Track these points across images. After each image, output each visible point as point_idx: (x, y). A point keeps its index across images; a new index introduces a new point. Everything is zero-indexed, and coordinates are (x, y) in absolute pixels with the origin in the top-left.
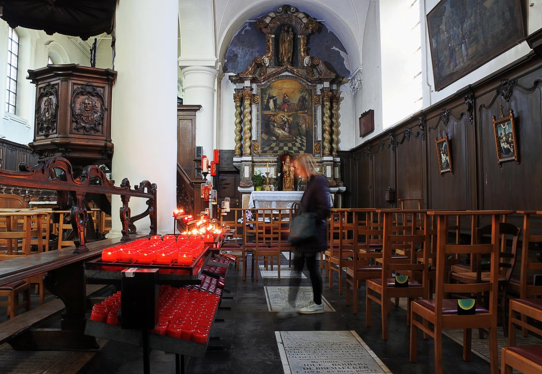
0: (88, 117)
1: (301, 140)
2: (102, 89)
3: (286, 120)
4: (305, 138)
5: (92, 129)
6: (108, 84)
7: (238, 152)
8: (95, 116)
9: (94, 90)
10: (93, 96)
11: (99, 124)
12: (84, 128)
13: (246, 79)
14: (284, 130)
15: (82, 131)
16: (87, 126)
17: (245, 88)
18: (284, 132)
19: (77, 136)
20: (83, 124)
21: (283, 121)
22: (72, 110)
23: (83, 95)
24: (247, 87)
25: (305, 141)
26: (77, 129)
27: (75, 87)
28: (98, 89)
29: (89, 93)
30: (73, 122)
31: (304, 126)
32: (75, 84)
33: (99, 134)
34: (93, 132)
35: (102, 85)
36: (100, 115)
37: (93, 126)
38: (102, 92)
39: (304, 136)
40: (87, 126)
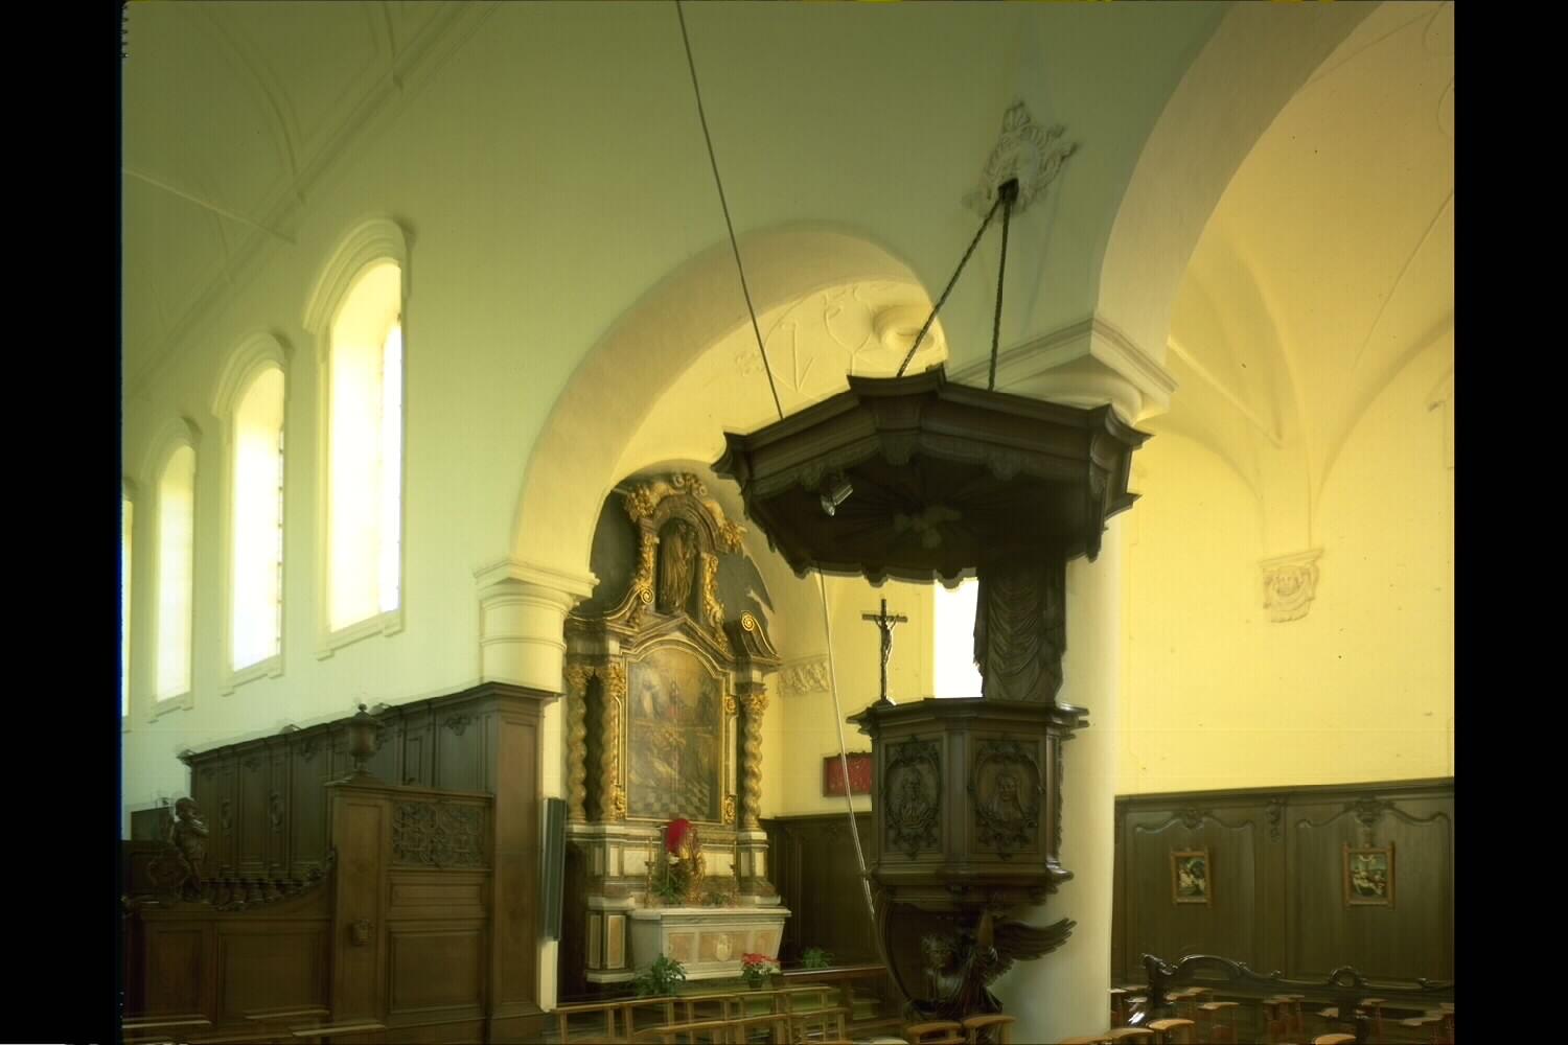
1: (701, 791)
3: (674, 743)
4: (707, 786)
14: (670, 764)
18: (669, 770)
21: (670, 744)
24: (615, 656)
25: (706, 792)
31: (705, 760)
39: (706, 783)
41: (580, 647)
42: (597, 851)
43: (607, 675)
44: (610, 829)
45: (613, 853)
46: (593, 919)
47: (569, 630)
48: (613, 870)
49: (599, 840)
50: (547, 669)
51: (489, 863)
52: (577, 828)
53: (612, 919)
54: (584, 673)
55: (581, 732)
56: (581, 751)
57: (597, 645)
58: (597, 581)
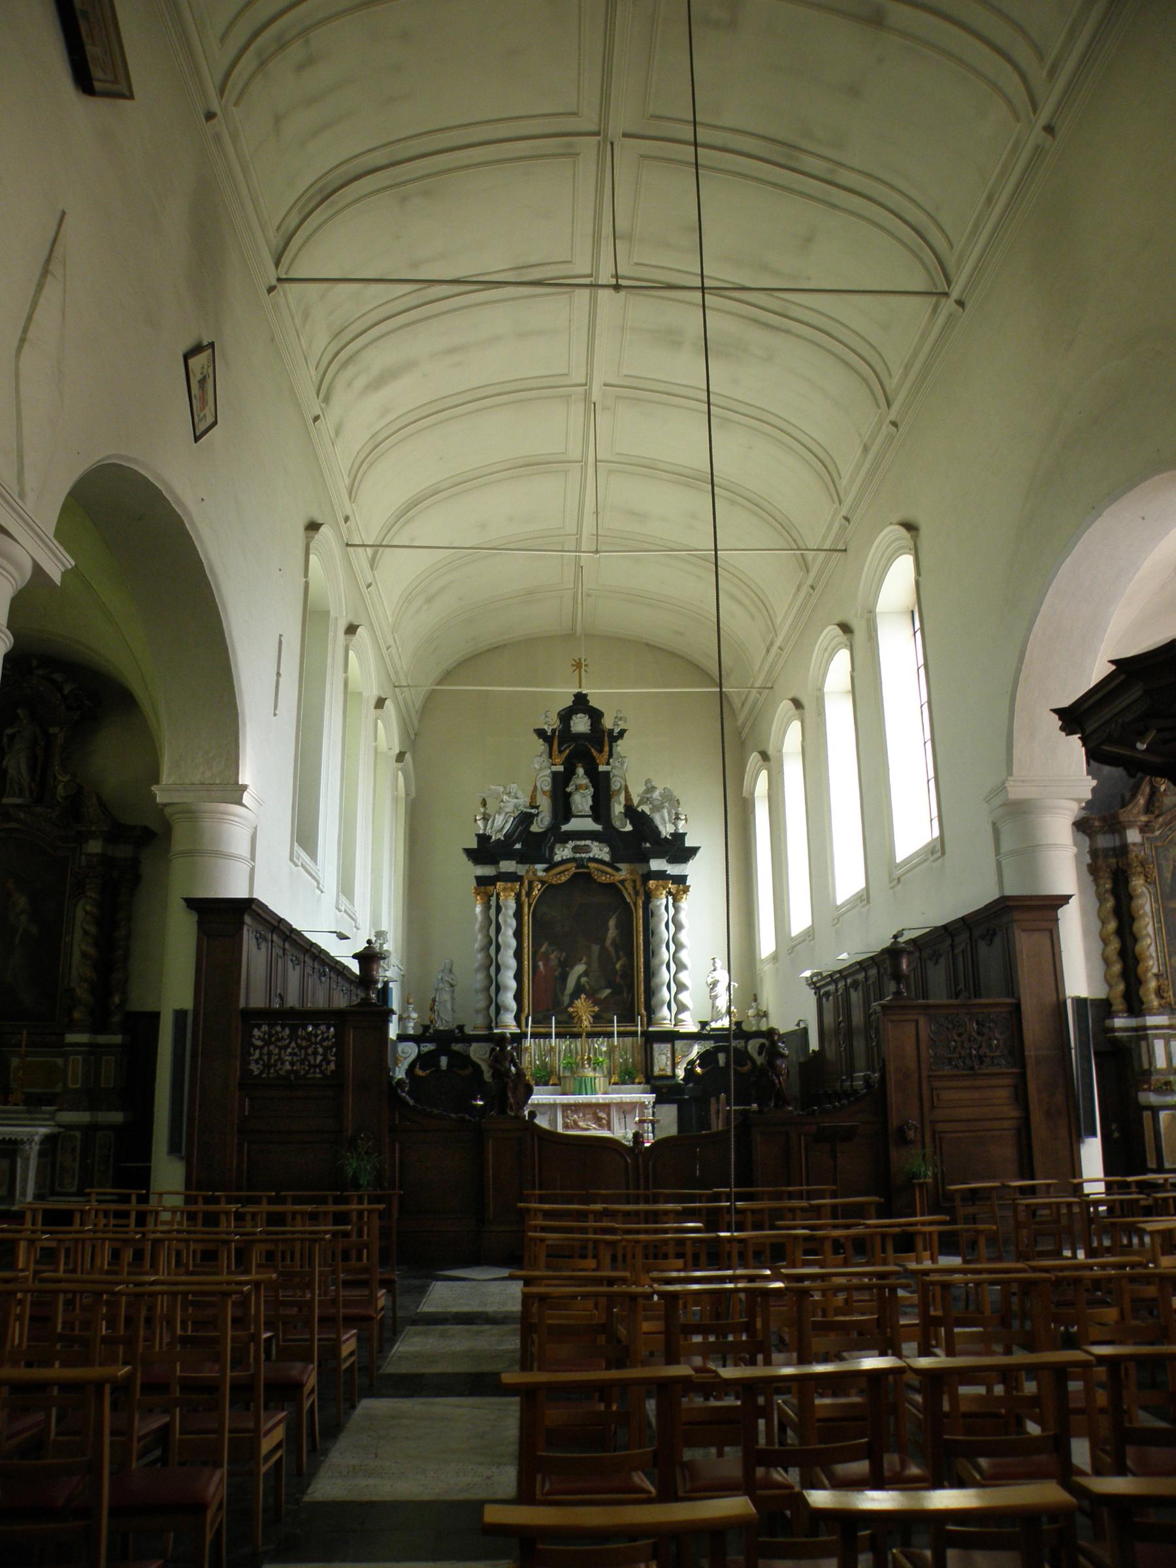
7: (1118, 1004)
13: (1131, 825)
17: (1131, 847)
24: (1134, 844)
41: (1104, 841)
42: (1143, 1044)
43: (1129, 865)
44: (1151, 1021)
45: (1159, 1046)
46: (1147, 1115)
47: (1081, 826)
48: (1161, 1063)
49: (1141, 1034)
50: (1063, 870)
51: (1021, 1062)
52: (1119, 1022)
53: (1163, 1115)
54: (1108, 866)
55: (1112, 925)
56: (1115, 945)
57: (1117, 837)
58: (1094, 783)
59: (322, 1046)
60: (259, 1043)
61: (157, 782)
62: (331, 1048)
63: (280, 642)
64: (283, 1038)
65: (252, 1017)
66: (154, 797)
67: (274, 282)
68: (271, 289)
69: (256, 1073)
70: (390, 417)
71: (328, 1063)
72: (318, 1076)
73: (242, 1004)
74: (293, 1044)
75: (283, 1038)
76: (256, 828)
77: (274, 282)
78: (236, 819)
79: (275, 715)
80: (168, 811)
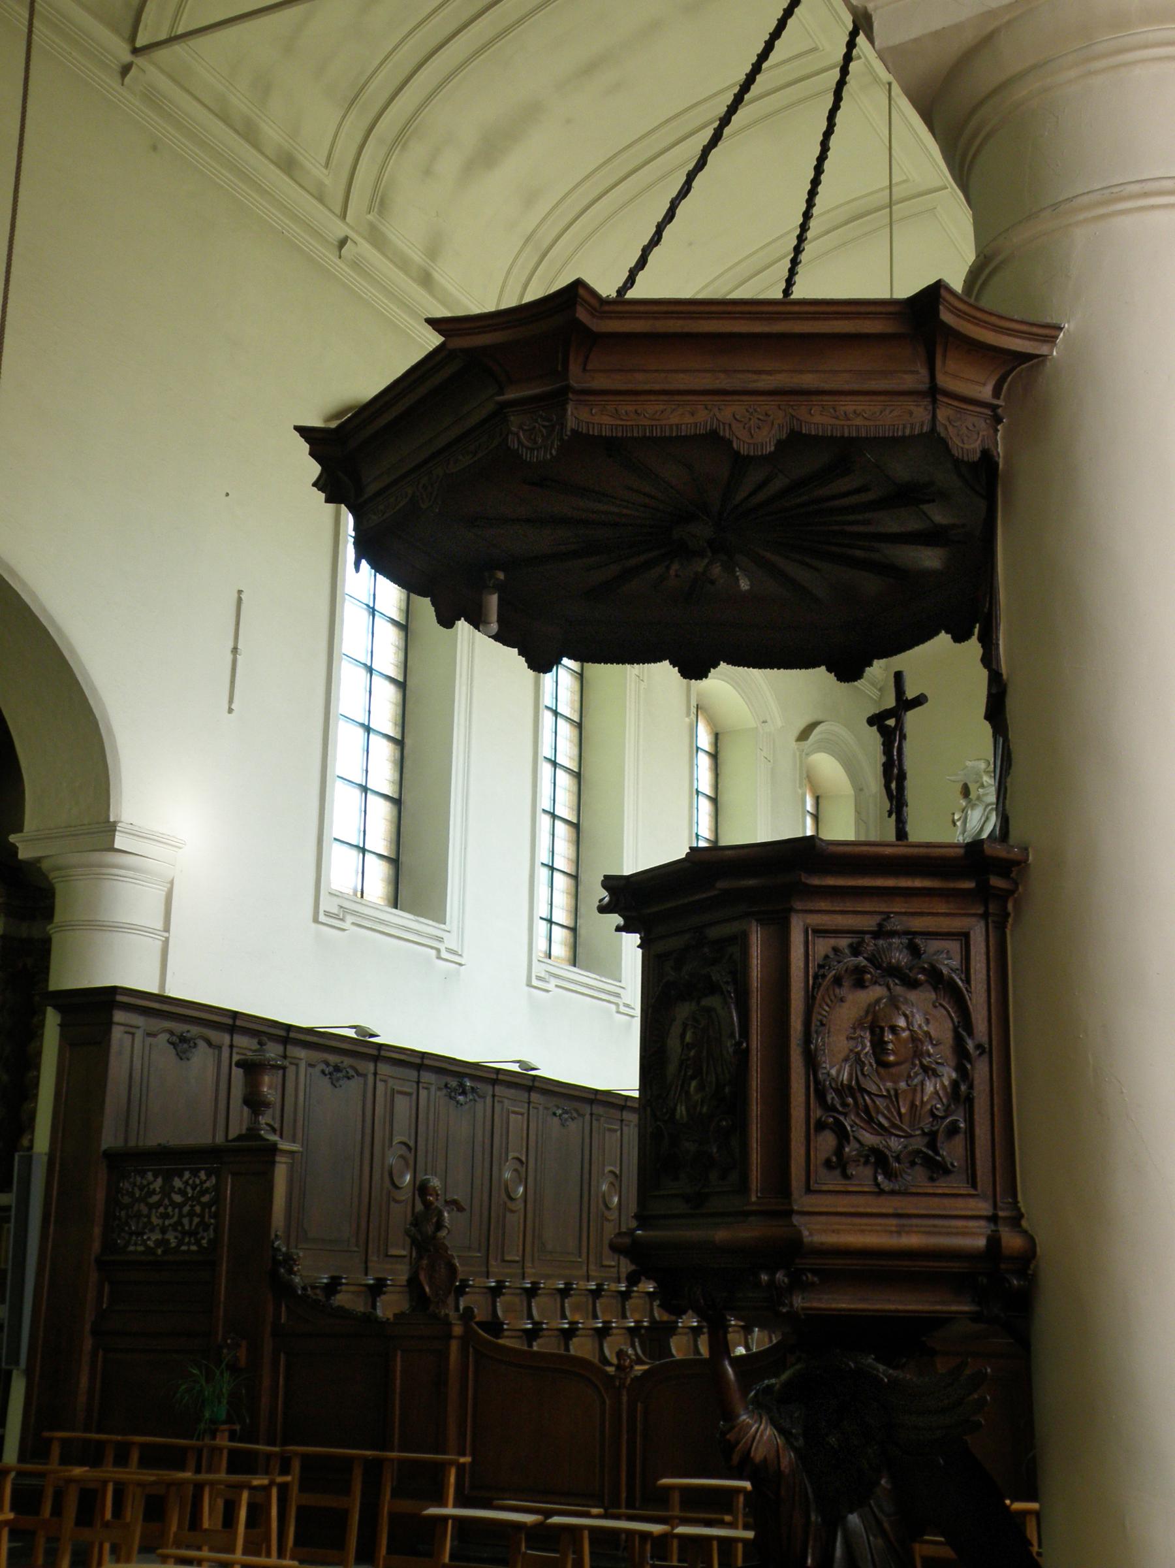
0: (893, 1097)
2: (954, 946)
5: (915, 1158)
6: (985, 916)
8: (929, 1088)
9: (914, 950)
10: (913, 984)
11: (953, 1130)
12: (879, 1159)
15: (863, 1174)
16: (895, 1144)
19: (843, 1204)
20: (869, 1138)
22: (811, 1061)
23: (860, 984)
26: (838, 1164)
27: (822, 947)
28: (934, 945)
29: (894, 972)
30: (821, 1126)
32: (820, 932)
33: (956, 1183)
34: (917, 1177)
35: (957, 924)
36: (955, 1084)
37: (919, 1143)
38: (955, 963)
40: (895, 1144)
59: (199, 1203)
60: (178, 1198)
61: (19, 828)
62: (209, 1205)
63: (240, 600)
64: (154, 1192)
65: (123, 1161)
66: (13, 850)
67: (127, 57)
68: (126, 70)
69: (173, 1245)
70: (543, 207)
71: (206, 1229)
72: (194, 1248)
73: (109, 1139)
74: (166, 1202)
75: (154, 1192)
76: (172, 883)
77: (127, 57)
78: (130, 874)
79: (230, 711)
80: (45, 865)
